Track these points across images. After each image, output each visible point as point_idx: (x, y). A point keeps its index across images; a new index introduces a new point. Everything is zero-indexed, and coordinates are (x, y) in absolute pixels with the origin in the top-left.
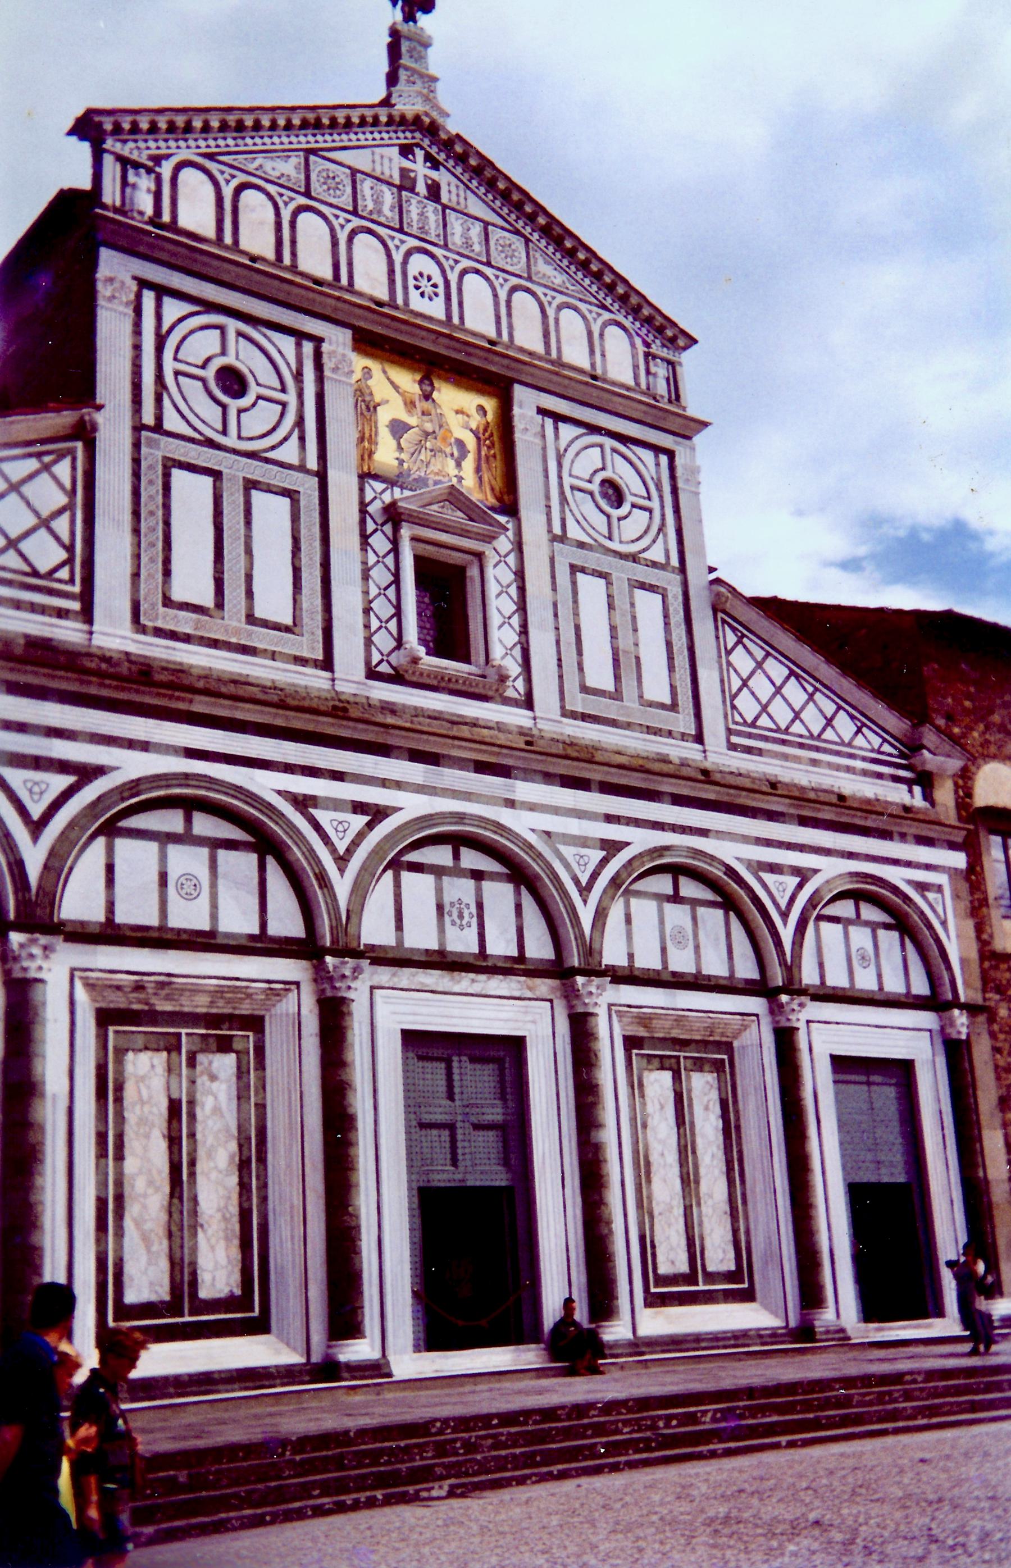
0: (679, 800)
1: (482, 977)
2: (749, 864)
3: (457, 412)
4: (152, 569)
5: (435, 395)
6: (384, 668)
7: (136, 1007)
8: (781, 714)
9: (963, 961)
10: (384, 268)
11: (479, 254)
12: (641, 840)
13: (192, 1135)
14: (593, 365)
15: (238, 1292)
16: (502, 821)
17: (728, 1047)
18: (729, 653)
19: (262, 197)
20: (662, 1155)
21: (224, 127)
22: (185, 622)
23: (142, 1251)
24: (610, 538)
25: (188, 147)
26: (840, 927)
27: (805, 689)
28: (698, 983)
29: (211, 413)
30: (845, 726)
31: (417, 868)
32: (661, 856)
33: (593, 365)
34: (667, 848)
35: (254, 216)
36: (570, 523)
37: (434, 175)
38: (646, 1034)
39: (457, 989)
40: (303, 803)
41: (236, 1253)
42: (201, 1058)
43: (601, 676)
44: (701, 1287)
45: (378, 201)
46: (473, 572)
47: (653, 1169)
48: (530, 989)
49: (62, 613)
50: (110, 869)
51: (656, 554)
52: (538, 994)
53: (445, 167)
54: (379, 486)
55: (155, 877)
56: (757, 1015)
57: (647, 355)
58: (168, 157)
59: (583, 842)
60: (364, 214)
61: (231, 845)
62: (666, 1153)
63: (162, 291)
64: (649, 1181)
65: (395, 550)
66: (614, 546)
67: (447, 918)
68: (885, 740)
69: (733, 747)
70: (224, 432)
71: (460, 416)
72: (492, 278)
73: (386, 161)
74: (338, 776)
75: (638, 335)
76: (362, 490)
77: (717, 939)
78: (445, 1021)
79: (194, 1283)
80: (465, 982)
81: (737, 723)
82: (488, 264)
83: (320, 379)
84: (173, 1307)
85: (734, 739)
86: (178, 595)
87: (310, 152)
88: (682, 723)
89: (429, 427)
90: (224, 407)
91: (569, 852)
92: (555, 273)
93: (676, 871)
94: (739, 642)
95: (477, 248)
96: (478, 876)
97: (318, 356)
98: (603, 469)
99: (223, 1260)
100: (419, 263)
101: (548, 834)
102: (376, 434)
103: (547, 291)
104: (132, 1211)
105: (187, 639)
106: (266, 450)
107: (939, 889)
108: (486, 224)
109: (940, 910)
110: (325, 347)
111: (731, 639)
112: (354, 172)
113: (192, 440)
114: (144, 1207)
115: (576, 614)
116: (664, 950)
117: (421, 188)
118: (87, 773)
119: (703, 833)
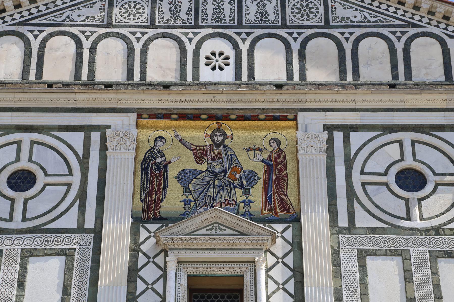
3: (248, 150)
5: (227, 142)
11: (276, 21)
19: (66, 39)
24: (409, 218)
25: (5, 22)
33: (395, 77)
35: (58, 53)
36: (359, 212)
46: (248, 278)
54: (153, 227)
60: (162, 24)
65: (164, 276)
66: (416, 223)
70: (10, 219)
71: (251, 153)
72: (286, 36)
76: (135, 233)
82: (284, 26)
83: (103, 159)
89: (218, 168)
92: (356, 13)
95: (272, 17)
97: (104, 139)
98: (402, 159)
102: (165, 186)
103: (393, 30)
106: (45, 224)
110: (108, 133)
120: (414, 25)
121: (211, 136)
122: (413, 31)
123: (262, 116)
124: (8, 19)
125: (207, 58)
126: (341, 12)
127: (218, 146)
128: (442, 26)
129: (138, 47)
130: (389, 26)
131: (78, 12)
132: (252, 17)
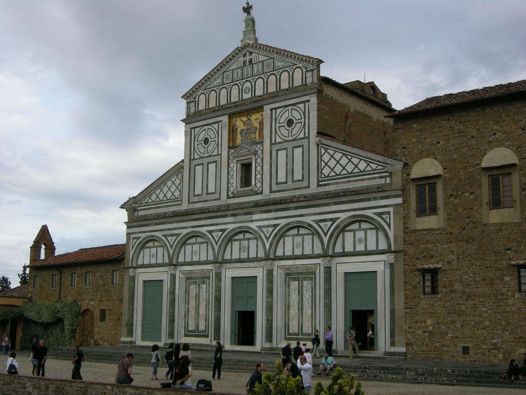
0: (296, 208)
1: (248, 263)
3: (255, 120)
4: (192, 190)
5: (251, 118)
6: (231, 195)
7: (191, 276)
8: (338, 169)
9: (395, 237)
10: (238, 92)
12: (283, 222)
13: (199, 300)
14: (289, 86)
15: (205, 330)
16: (250, 226)
17: (314, 273)
18: (322, 156)
20: (294, 303)
21: (206, 81)
22: (196, 199)
23: (191, 321)
26: (352, 233)
27: (348, 158)
28: (303, 257)
29: (202, 150)
30: (362, 165)
31: (236, 240)
32: (289, 225)
34: (291, 223)
35: (212, 98)
36: (277, 137)
37: (251, 57)
38: (291, 272)
39: (242, 267)
40: (210, 232)
41: (204, 322)
42: (201, 285)
43: (282, 178)
44: (300, 337)
45: (237, 75)
47: (290, 307)
48: (258, 264)
49: (179, 205)
50: (185, 251)
51: (302, 136)
52: (260, 266)
53: (254, 53)
55: (191, 252)
56: (320, 264)
57: (306, 72)
58: (197, 96)
59: (268, 226)
61: (203, 243)
62: (295, 302)
63: (195, 128)
64: (289, 309)
66: (290, 138)
67: (241, 251)
68: (378, 165)
69: (321, 186)
73: (240, 62)
74: (217, 224)
75: (304, 67)
77: (309, 244)
78: (240, 274)
79: (198, 327)
81: (323, 178)
82: (263, 73)
83: (222, 131)
84: (194, 331)
85: (321, 183)
86: (196, 194)
87: (223, 73)
88: (304, 184)
90: (205, 147)
91: (264, 230)
93: (298, 227)
94: (326, 151)
95: (260, 71)
96: (249, 239)
99: (203, 323)
100: (248, 85)
101: (260, 226)
104: (190, 314)
105: (197, 202)
107: (389, 213)
108: (263, 61)
109: (388, 220)
111: (323, 151)
112: (232, 70)
113: (199, 159)
114: (192, 313)
115: (277, 163)
116: (293, 249)
117: (248, 63)
118: (178, 235)
119: (302, 216)
120: (295, 65)
121: (247, 117)
122: (295, 67)
123: (257, 108)
124: (201, 89)
125: (245, 90)
127: (249, 120)
128: (302, 63)
129: (229, 90)
130: (288, 67)
131: (216, 82)
132: (255, 72)
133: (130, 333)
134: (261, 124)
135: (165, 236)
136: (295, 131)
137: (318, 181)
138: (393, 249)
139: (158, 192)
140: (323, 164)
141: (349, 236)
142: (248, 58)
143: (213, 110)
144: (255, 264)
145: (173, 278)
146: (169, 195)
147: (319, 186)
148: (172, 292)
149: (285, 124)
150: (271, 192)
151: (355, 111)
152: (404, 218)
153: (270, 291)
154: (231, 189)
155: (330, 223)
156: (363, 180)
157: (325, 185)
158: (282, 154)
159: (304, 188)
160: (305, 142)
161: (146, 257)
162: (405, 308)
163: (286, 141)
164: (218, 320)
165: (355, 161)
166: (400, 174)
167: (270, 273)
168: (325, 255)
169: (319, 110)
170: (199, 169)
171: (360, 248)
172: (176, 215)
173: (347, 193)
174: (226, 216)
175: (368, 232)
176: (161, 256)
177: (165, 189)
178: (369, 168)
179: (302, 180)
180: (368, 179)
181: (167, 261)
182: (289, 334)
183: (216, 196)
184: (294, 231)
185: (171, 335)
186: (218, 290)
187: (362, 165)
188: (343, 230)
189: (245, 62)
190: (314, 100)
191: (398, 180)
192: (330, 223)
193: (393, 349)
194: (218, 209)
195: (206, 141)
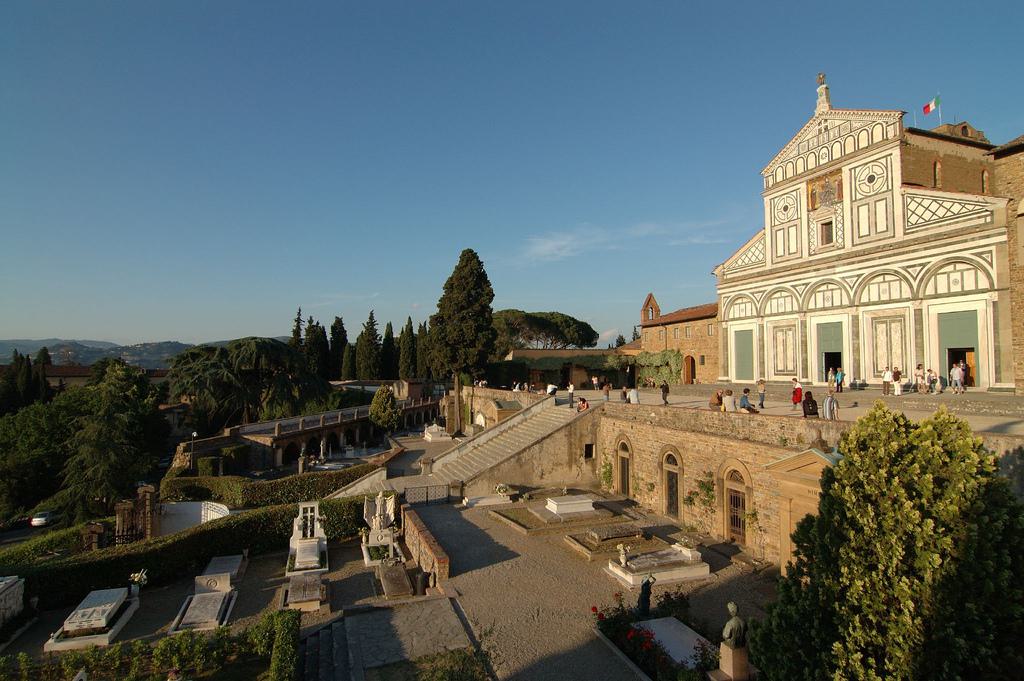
0: (880, 258)
2: (903, 268)
8: (927, 215)
9: (999, 275)
12: (867, 272)
17: (904, 316)
22: (779, 260)
29: (782, 217)
43: (864, 231)
51: (885, 189)
66: (872, 193)
69: (908, 234)
80: (829, 312)
96: (832, 290)
107: (991, 252)
111: (909, 200)
126: (855, 125)
133: (726, 373)
134: (840, 185)
135: (753, 294)
136: (876, 187)
137: (905, 229)
138: (996, 288)
139: (743, 258)
140: (910, 213)
141: (942, 280)
142: (823, 125)
143: (791, 180)
144: (840, 311)
145: (761, 327)
146: (753, 259)
147: (905, 234)
148: (761, 340)
149: (866, 181)
150: (853, 246)
151: (945, 155)
152: (1010, 255)
153: (856, 335)
154: (813, 247)
155: (919, 268)
156: (957, 222)
157: (913, 232)
158: (864, 210)
159: (889, 238)
160: (888, 195)
161: (735, 312)
162: (1014, 345)
163: (867, 197)
164: (805, 361)
165: (947, 205)
166: (1004, 211)
167: (855, 319)
168: (915, 298)
169: (902, 161)
170: (780, 233)
171: (956, 288)
172: (760, 274)
173: (938, 237)
174: (809, 271)
175: (965, 273)
176: (750, 309)
177: (750, 255)
178: (964, 210)
179: (887, 231)
180: (965, 221)
181: (755, 314)
182: (878, 371)
183: (798, 255)
184: (880, 279)
185: (762, 374)
186: (804, 335)
187: (956, 208)
188: (935, 274)
189: (820, 131)
190: (896, 152)
191: (1001, 218)
192: (919, 268)
193: (998, 385)
194: (800, 266)
195: (786, 208)
